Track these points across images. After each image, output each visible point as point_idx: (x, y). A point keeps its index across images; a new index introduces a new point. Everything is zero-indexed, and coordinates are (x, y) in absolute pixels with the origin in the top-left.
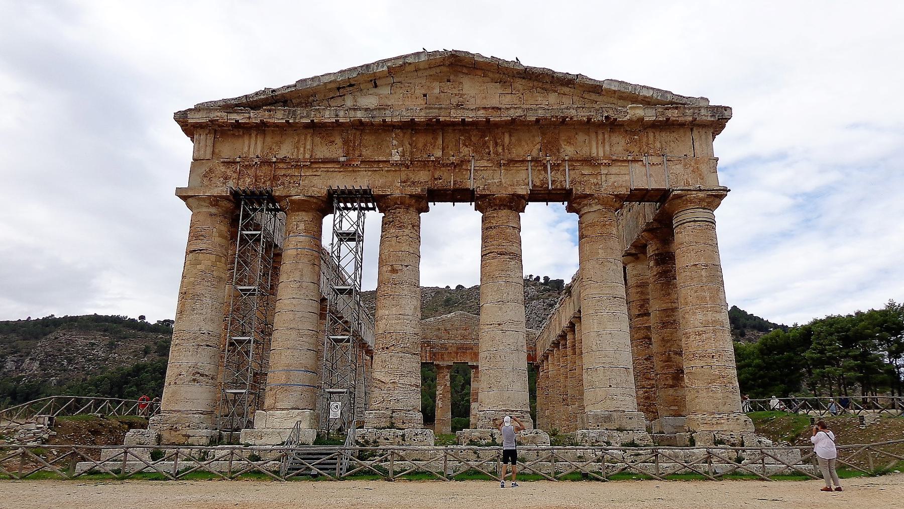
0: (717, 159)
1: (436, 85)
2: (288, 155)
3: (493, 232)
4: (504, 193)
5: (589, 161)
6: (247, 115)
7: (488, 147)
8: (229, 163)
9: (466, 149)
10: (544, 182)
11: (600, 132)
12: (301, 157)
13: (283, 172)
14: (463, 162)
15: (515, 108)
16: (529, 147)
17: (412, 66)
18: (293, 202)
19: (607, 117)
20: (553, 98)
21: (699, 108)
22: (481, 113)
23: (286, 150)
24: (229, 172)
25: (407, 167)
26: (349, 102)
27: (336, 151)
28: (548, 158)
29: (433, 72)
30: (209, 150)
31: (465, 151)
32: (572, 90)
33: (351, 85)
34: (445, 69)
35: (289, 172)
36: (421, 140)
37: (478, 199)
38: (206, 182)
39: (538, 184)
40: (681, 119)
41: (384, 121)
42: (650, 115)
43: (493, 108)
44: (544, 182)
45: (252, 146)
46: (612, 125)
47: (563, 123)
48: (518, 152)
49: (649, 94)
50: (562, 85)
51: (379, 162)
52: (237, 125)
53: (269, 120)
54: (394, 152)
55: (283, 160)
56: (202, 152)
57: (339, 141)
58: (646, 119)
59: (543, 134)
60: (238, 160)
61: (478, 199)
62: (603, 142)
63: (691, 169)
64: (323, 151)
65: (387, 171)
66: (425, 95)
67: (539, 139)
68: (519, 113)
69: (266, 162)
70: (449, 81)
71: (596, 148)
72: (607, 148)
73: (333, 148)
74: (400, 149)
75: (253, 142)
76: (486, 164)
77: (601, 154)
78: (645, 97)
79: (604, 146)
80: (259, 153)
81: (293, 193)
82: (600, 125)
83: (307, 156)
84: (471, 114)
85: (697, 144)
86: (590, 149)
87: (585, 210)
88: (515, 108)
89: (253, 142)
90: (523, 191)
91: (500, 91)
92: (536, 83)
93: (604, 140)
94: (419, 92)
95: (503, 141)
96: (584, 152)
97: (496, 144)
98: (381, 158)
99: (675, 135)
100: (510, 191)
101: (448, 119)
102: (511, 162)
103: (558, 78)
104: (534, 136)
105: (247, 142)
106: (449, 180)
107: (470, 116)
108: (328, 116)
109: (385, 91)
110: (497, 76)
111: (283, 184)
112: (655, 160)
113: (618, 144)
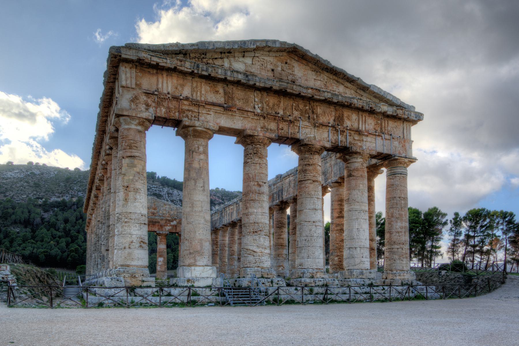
0: (413, 141)
1: (279, 64)
2: (189, 95)
3: (311, 168)
4: (318, 145)
5: (359, 132)
7: (308, 114)
8: (148, 94)
10: (337, 141)
11: (364, 116)
12: (199, 99)
13: (186, 108)
14: (296, 120)
15: (328, 92)
16: (327, 116)
18: (195, 131)
19: (371, 108)
21: (411, 111)
22: (310, 91)
23: (186, 92)
24: (150, 101)
25: (264, 118)
28: (339, 127)
29: (278, 54)
30: (134, 82)
31: (296, 113)
32: (352, 86)
33: (229, 52)
34: (285, 54)
35: (191, 108)
36: (272, 100)
37: (302, 145)
38: (133, 106)
39: (334, 142)
40: (403, 116)
41: (255, 84)
42: (390, 110)
43: (316, 89)
44: (337, 141)
45: (165, 85)
46: (371, 112)
47: (350, 106)
48: (323, 119)
49: (391, 98)
50: (348, 81)
53: (181, 68)
54: (256, 106)
55: (187, 99)
56: (128, 82)
57: (221, 91)
58: (389, 113)
59: (336, 110)
60: (156, 93)
61: (302, 145)
62: (365, 122)
66: (273, 70)
67: (333, 113)
68: (329, 95)
69: (176, 98)
70: (286, 63)
73: (218, 96)
74: (260, 105)
75: (165, 82)
76: (307, 124)
77: (364, 129)
78: (388, 100)
79: (365, 125)
80: (170, 90)
81: (197, 124)
82: (366, 111)
84: (305, 91)
85: (405, 131)
86: (359, 124)
87: (354, 160)
88: (328, 92)
89: (165, 82)
91: (315, 77)
92: (334, 77)
93: (365, 120)
94: (270, 67)
96: (355, 126)
97: (313, 113)
98: (249, 110)
99: (396, 124)
100: (322, 144)
101: (291, 91)
102: (322, 125)
103: (348, 78)
104: (331, 111)
105: (160, 80)
106: (287, 130)
109: (248, 61)
110: (314, 67)
111: (187, 116)
112: (387, 137)
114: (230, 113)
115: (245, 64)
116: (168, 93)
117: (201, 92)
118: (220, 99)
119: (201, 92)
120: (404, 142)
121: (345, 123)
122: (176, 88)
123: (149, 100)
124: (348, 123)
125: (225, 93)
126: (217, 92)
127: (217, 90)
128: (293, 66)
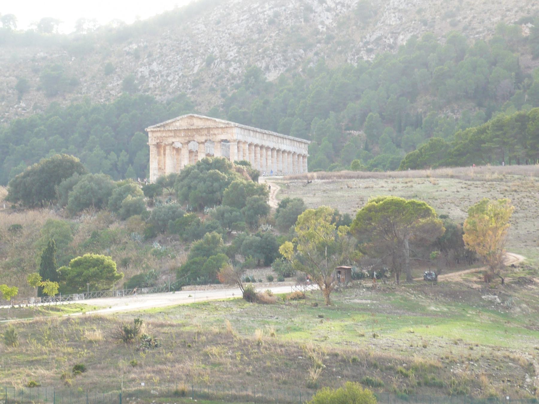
5: (215, 134)
8: (155, 138)
20: (209, 121)
23: (164, 134)
26: (174, 124)
27: (173, 134)
31: (194, 133)
48: (203, 133)
64: (171, 134)
71: (216, 132)
90: (203, 141)
102: (202, 135)
107: (194, 128)
108: (170, 129)
109: (180, 121)
113: (220, 130)
124: (211, 132)
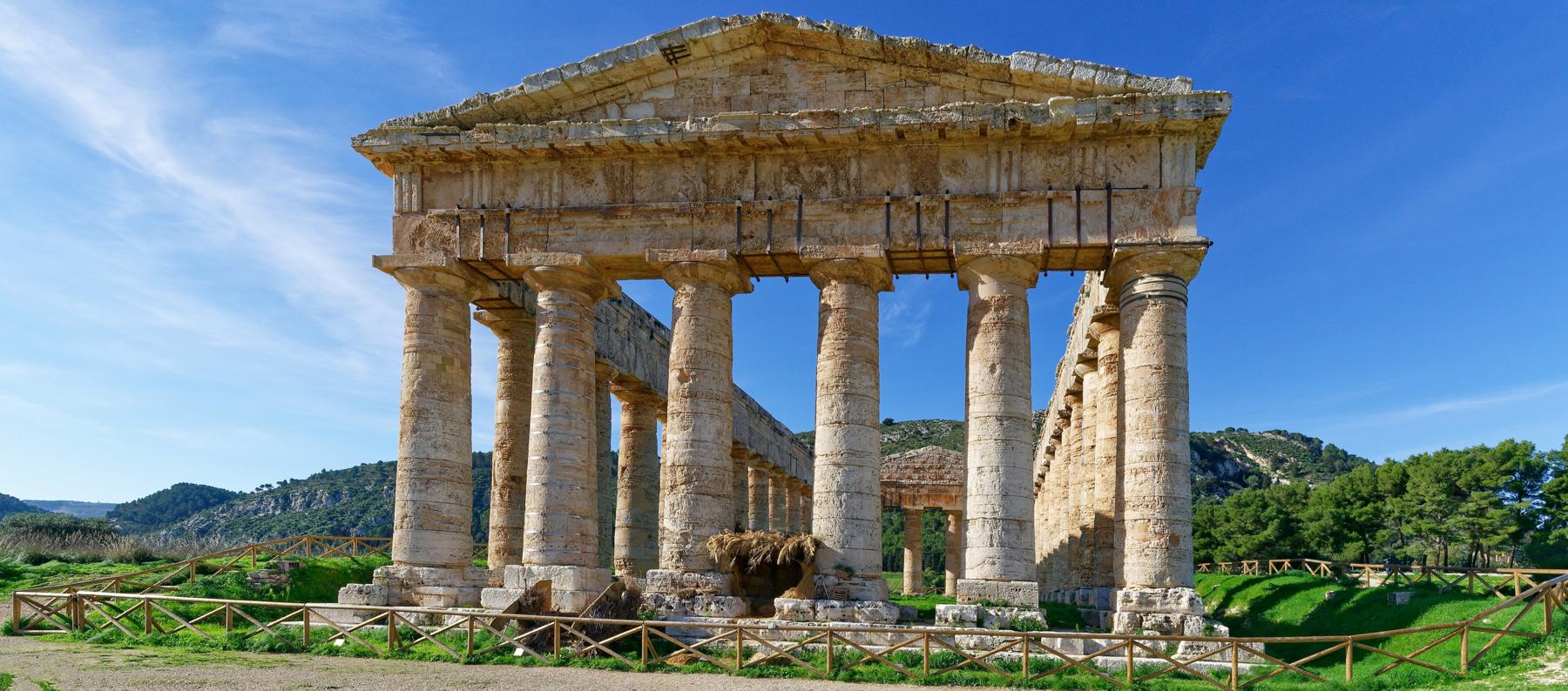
6: (455, 139)
9: (792, 188)
11: (1004, 151)
12: (546, 205)
17: (701, 45)
23: (524, 196)
32: (963, 79)
51: (658, 211)
52: (451, 158)
57: (600, 179)
62: (1009, 170)
63: (1150, 209)
65: (673, 226)
66: (728, 99)
72: (1015, 178)
73: (592, 191)
75: (476, 185)
79: (1009, 177)
80: (485, 201)
81: (534, 261)
83: (555, 204)
85: (1167, 167)
91: (846, 87)
95: (847, 173)
105: (467, 185)
108: (574, 136)
110: (841, 59)
114: (618, 223)
115: (658, 100)
116: (483, 207)
117: (550, 191)
118: (599, 193)
119: (550, 191)
120: (1161, 199)
121: (942, 184)
122: (503, 194)
123: (445, 229)
125: (610, 180)
126: (590, 182)
127: (590, 177)
128: (783, 75)
